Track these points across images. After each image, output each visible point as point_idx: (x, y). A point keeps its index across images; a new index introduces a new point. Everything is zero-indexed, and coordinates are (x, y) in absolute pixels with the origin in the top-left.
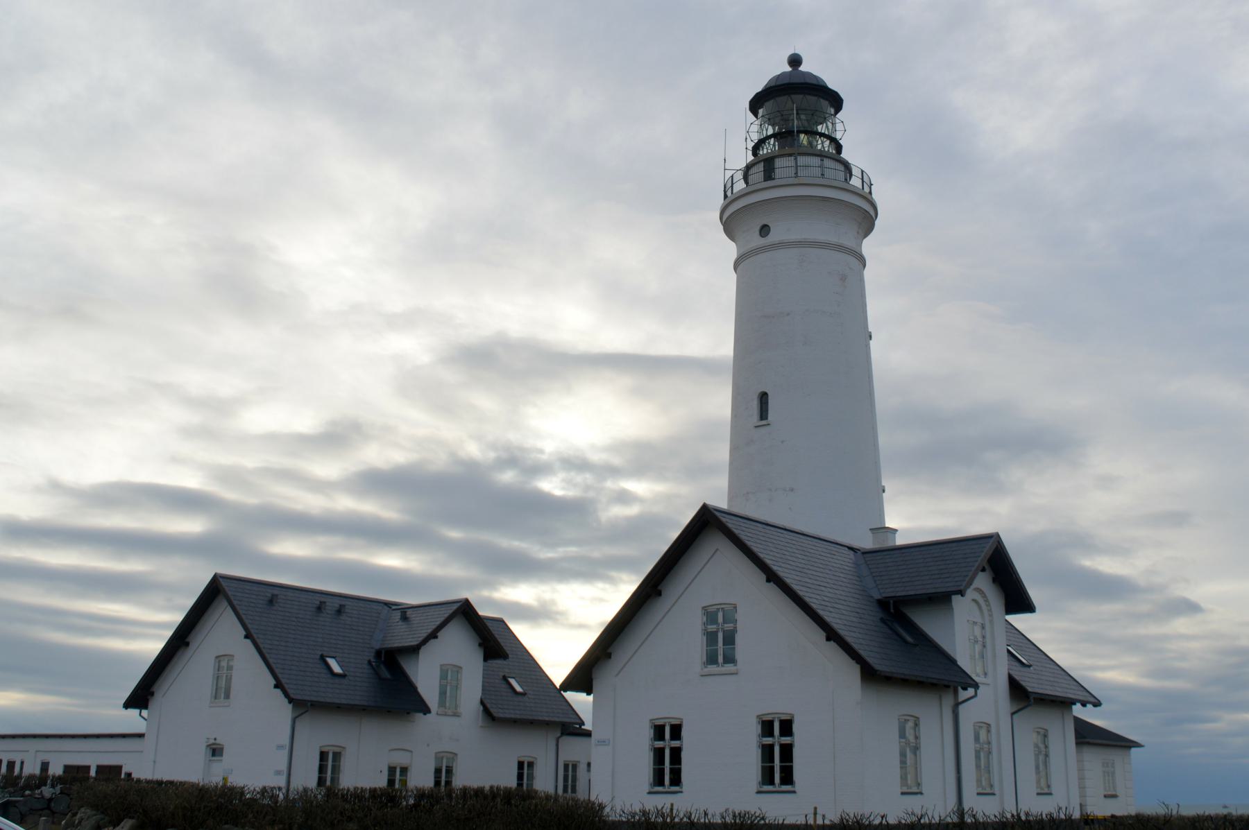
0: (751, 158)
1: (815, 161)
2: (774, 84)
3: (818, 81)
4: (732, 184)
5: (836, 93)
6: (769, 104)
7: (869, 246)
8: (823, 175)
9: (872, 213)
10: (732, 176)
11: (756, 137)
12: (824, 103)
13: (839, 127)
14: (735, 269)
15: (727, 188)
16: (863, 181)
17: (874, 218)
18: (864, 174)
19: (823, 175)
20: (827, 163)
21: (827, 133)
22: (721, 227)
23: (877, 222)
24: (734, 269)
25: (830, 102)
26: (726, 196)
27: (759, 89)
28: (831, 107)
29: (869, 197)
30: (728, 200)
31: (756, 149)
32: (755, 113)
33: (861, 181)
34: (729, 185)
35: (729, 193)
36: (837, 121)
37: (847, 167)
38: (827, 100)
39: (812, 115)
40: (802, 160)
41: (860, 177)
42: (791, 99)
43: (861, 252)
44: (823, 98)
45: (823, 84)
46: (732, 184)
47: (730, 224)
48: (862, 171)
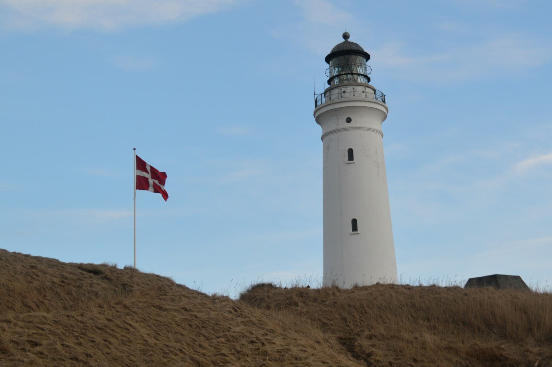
2: (335, 51)
8: (354, 95)
10: (316, 99)
12: (360, 59)
13: (368, 68)
14: (322, 140)
17: (386, 112)
19: (354, 95)
21: (363, 74)
27: (329, 53)
30: (317, 108)
31: (329, 82)
32: (329, 63)
38: (362, 56)
40: (344, 89)
42: (345, 58)
44: (360, 56)
45: (361, 50)
47: (319, 119)
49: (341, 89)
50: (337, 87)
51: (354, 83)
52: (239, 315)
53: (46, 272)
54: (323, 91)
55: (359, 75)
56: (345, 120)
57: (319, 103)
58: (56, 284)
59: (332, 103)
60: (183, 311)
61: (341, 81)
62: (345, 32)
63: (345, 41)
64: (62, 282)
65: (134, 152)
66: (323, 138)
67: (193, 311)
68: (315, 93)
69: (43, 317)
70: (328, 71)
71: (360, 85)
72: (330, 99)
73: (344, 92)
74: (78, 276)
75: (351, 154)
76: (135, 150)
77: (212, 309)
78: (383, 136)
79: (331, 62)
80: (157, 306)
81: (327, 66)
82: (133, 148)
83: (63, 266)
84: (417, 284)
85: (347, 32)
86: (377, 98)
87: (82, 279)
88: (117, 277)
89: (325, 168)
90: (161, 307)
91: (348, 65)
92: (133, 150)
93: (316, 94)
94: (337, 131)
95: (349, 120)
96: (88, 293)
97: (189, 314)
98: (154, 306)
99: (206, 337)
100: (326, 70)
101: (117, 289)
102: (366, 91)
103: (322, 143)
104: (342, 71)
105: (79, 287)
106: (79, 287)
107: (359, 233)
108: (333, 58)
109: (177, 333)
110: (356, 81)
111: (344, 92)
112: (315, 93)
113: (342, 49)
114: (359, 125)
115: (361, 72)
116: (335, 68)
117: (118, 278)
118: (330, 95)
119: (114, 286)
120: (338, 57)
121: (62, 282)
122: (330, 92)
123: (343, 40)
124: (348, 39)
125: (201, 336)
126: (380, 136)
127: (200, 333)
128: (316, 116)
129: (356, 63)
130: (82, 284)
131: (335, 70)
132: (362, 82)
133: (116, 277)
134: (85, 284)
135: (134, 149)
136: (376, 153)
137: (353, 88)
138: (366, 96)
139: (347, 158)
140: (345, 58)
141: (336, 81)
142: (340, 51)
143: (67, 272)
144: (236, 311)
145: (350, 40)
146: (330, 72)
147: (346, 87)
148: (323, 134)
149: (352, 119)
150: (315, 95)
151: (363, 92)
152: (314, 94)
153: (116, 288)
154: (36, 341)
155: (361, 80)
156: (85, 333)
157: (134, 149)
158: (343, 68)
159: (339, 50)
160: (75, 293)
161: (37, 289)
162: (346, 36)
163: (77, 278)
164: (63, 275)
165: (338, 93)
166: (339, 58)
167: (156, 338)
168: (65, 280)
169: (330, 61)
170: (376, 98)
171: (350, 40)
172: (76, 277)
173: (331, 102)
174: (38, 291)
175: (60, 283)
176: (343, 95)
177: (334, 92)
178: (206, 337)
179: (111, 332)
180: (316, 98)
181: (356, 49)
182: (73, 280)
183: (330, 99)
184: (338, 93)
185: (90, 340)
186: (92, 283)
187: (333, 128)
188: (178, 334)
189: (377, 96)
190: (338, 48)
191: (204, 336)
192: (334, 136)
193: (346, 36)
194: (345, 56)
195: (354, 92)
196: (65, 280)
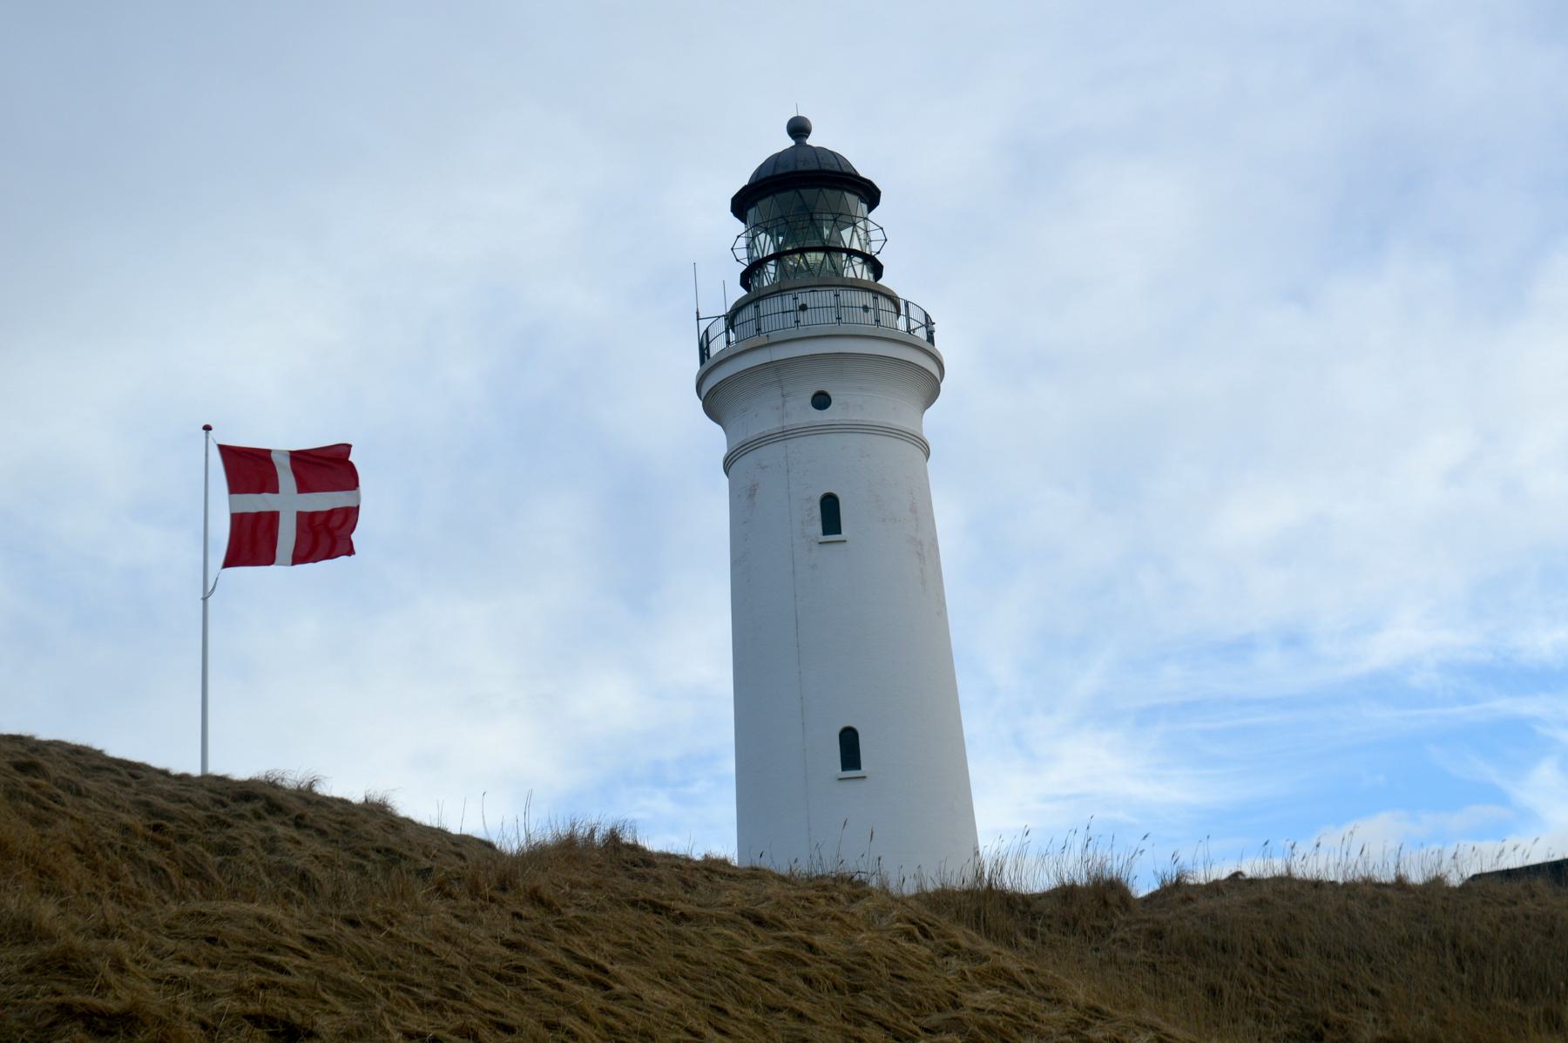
1: (825, 297)
2: (770, 174)
7: (932, 422)
8: (839, 318)
10: (707, 331)
12: (851, 199)
13: (875, 235)
14: (727, 470)
17: (939, 379)
19: (839, 318)
23: (942, 385)
24: (725, 471)
26: (702, 362)
28: (862, 202)
29: (928, 346)
30: (708, 364)
31: (746, 279)
32: (743, 220)
36: (871, 227)
39: (835, 220)
40: (805, 298)
43: (921, 434)
46: (708, 343)
49: (796, 298)
50: (778, 291)
51: (837, 281)
52: (948, 947)
53: (84, 792)
54: (724, 309)
55: (851, 253)
57: (717, 346)
58: (136, 835)
59: (766, 343)
60: (747, 922)
61: (783, 272)
63: (797, 143)
64: (156, 828)
65: (207, 437)
66: (728, 464)
67: (786, 927)
68: (698, 313)
69: (260, 919)
70: (742, 242)
71: (856, 285)
72: (759, 330)
73: (803, 308)
74: (206, 809)
75: (830, 511)
76: (210, 432)
77: (845, 922)
78: (928, 455)
79: (751, 212)
80: (644, 901)
81: (740, 227)
82: (202, 426)
83: (133, 771)
84: (1388, 877)
85: (800, 115)
86: (914, 330)
87: (230, 820)
88: (342, 823)
89: (736, 563)
90: (662, 907)
92: (204, 431)
93: (701, 316)
94: (785, 435)
95: (821, 401)
96: (269, 875)
97: (775, 938)
98: (634, 904)
99: (888, 1029)
100: (738, 237)
101: (369, 867)
102: (876, 305)
103: (725, 481)
104: (785, 243)
105: (222, 849)
106: (222, 849)
107: (867, 774)
108: (761, 198)
109: (779, 1010)
110: (838, 272)
111: (803, 308)
112: (698, 313)
113: (791, 169)
115: (856, 246)
117: (345, 827)
118: (758, 318)
119: (348, 853)
120: (777, 196)
121: (156, 828)
122: (757, 307)
123: (790, 142)
124: (807, 137)
125: (870, 1024)
126: (922, 456)
127: (861, 1013)
128: (705, 389)
129: (841, 214)
130: (235, 839)
132: (859, 277)
133: (337, 826)
134: (248, 841)
136: (913, 510)
137: (837, 295)
138: (878, 321)
139: (818, 527)
140: (799, 193)
142: (787, 174)
143: (160, 793)
144: (926, 934)
145: (811, 141)
146: (748, 247)
147: (814, 291)
148: (728, 450)
150: (700, 321)
151: (866, 309)
152: (696, 318)
153: (365, 863)
154: (288, 1016)
155: (857, 270)
156: (458, 989)
157: (207, 428)
158: (790, 235)
159: (780, 171)
160: (219, 872)
161: (76, 849)
162: (799, 129)
163: (208, 817)
164: (147, 804)
165: (780, 311)
166: (780, 196)
167: (721, 1026)
168: (164, 822)
169: (749, 208)
170: (908, 327)
171: (811, 141)
172: (201, 812)
173: (762, 340)
174: (79, 855)
175: (150, 833)
177: (767, 306)
178: (888, 1029)
179: (549, 990)
180: (702, 331)
181: (837, 168)
182: (195, 822)
183: (759, 330)
184: (783, 312)
185: (491, 1021)
186: (273, 839)
187: (771, 424)
188: (781, 1015)
189: (913, 325)
191: (880, 1024)
192: (768, 453)
193: (799, 129)
194: (802, 191)
195: (838, 307)
196: (164, 822)
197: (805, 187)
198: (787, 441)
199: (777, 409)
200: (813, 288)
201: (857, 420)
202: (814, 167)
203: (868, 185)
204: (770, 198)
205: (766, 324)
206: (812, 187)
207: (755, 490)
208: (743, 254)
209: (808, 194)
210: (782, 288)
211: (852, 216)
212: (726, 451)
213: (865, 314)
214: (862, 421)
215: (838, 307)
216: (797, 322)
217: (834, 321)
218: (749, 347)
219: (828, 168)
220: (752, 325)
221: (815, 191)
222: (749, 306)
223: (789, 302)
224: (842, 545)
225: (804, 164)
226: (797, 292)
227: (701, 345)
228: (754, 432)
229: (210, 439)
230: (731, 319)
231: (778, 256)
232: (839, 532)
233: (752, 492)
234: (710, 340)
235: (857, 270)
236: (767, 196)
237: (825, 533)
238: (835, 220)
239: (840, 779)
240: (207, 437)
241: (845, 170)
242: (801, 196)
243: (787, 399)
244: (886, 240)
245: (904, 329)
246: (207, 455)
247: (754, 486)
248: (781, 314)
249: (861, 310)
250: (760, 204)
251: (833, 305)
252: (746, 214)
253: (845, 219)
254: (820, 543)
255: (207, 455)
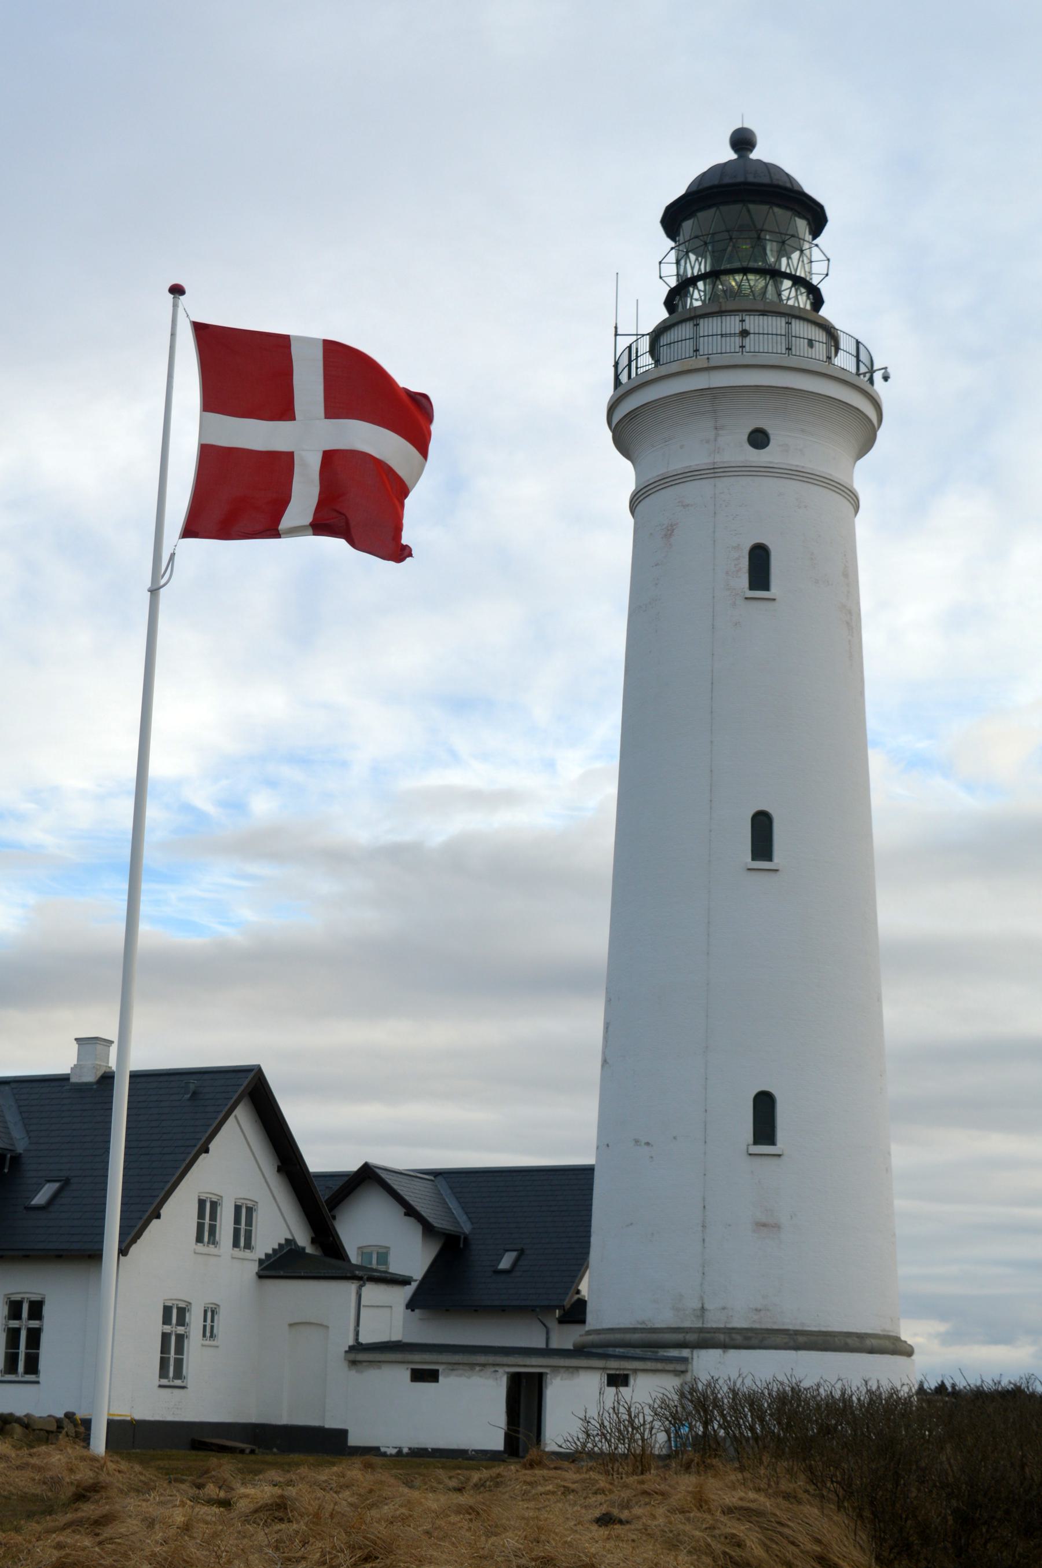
0: (664, 314)
1: (777, 324)
2: (716, 182)
3: (791, 182)
4: (637, 357)
5: (821, 208)
6: (707, 218)
8: (789, 349)
9: (874, 418)
10: (630, 347)
11: (673, 282)
13: (818, 268)
14: (633, 508)
15: (620, 370)
16: (858, 361)
18: (861, 348)
19: (789, 349)
20: (800, 328)
22: (609, 434)
25: (809, 224)
30: (621, 390)
33: (854, 360)
34: (624, 362)
35: (624, 378)
37: (831, 333)
40: (753, 323)
41: (854, 353)
43: (852, 486)
45: (799, 189)
48: (858, 343)
49: (742, 321)
50: (715, 309)
54: (649, 327)
56: (745, 437)
62: (740, 126)
63: (740, 157)
65: (175, 306)
68: (616, 328)
70: (672, 257)
72: (697, 351)
73: (744, 333)
79: (688, 227)
85: (746, 126)
91: (759, 238)
93: (619, 332)
94: (715, 472)
95: (759, 439)
112: (616, 328)
113: (740, 179)
114: (795, 461)
116: (687, 253)
118: (696, 338)
120: (721, 207)
122: (697, 325)
123: (732, 156)
124: (751, 151)
128: (617, 417)
131: (688, 261)
135: (177, 290)
136: (846, 575)
139: (744, 580)
141: (697, 298)
145: (754, 155)
148: (636, 488)
149: (772, 437)
150: (618, 337)
152: (614, 333)
155: (798, 300)
159: (727, 180)
162: (742, 141)
166: (724, 209)
171: (754, 155)
173: (701, 362)
176: (747, 341)
181: (788, 185)
187: (699, 459)
190: (699, 185)
192: (691, 490)
193: (742, 141)
194: (751, 206)
197: (754, 202)
198: (717, 479)
199: (708, 442)
200: (764, 313)
201: (797, 466)
202: (765, 180)
203: (819, 210)
204: (713, 210)
205: (705, 346)
206: (762, 202)
207: (673, 530)
208: (670, 270)
209: (759, 210)
210: (723, 309)
211: (800, 239)
212: (633, 488)
213: (810, 349)
214: (803, 467)
215: (788, 335)
216: (742, 347)
217: (784, 352)
218: (685, 368)
219: (781, 183)
220: (689, 346)
221: (765, 208)
222: (688, 323)
223: (732, 324)
224: (770, 604)
225: (755, 177)
226: (744, 314)
227: (616, 365)
228: (677, 465)
229: (180, 310)
230: (656, 336)
231: (713, 275)
232: (766, 587)
233: (669, 532)
234: (639, 355)
235: (798, 300)
236: (709, 207)
237: (752, 587)
238: (783, 242)
239: (749, 869)
240: (175, 306)
241: (796, 188)
242: (749, 211)
243: (720, 432)
244: (827, 275)
245: (854, 370)
246: (173, 335)
247: (672, 525)
248: (719, 337)
249: (806, 341)
250: (700, 215)
251: (783, 333)
252: (680, 226)
253: (788, 243)
254: (746, 598)
255: (173, 335)
